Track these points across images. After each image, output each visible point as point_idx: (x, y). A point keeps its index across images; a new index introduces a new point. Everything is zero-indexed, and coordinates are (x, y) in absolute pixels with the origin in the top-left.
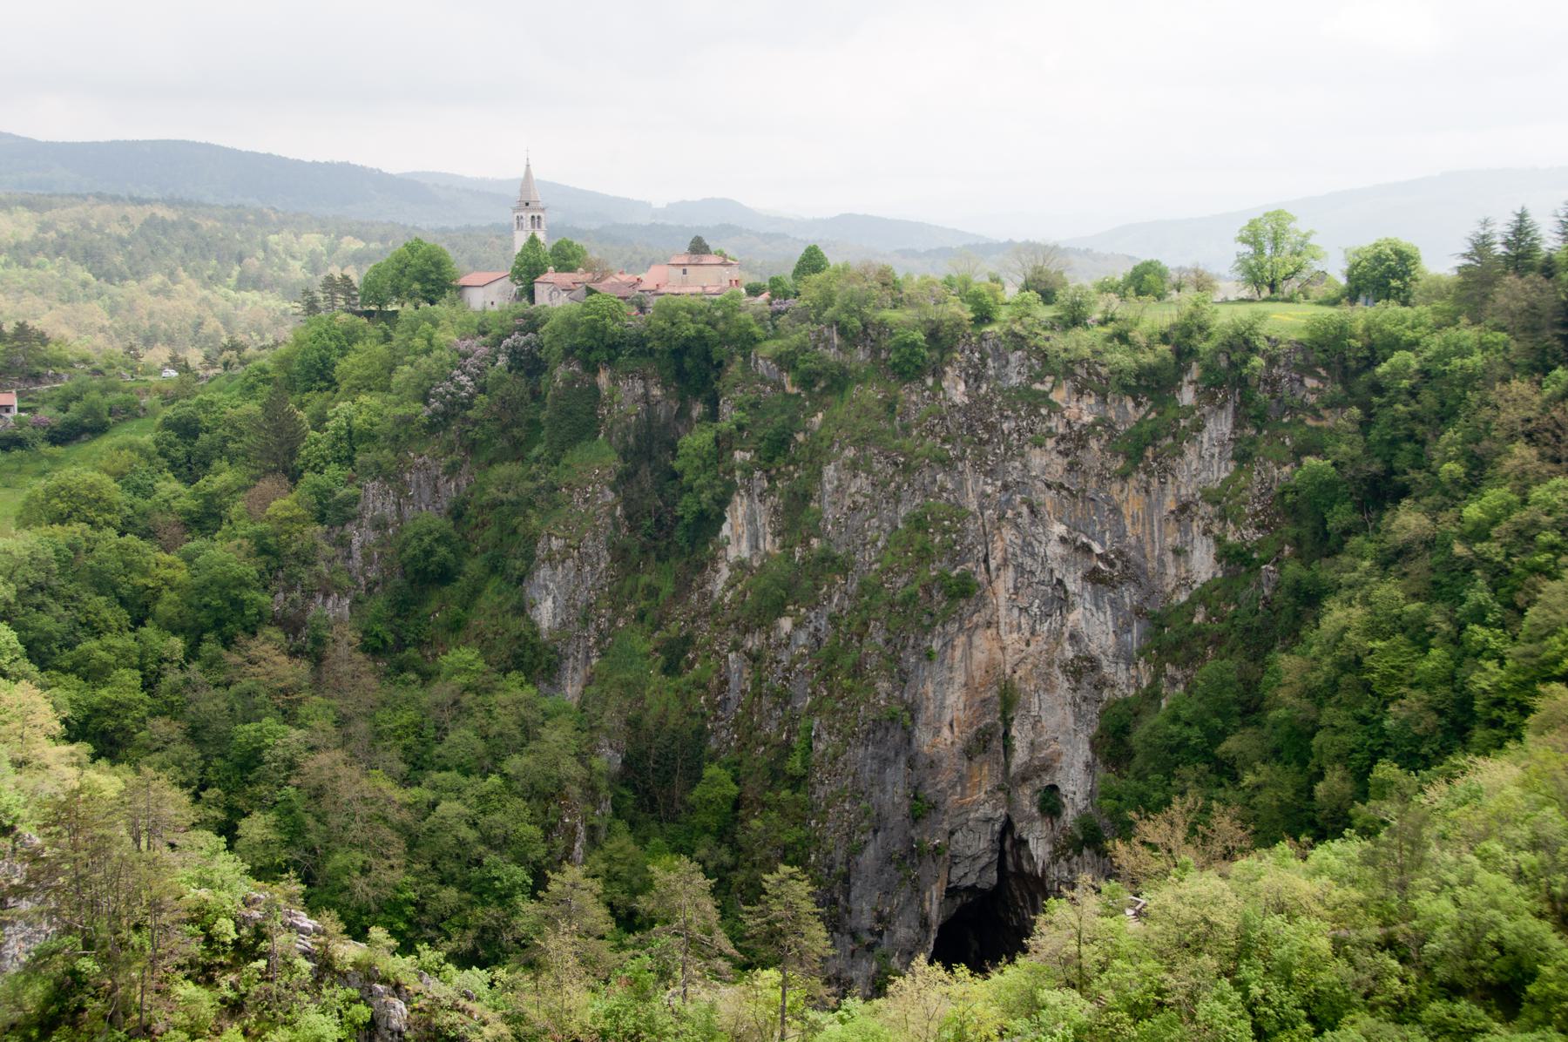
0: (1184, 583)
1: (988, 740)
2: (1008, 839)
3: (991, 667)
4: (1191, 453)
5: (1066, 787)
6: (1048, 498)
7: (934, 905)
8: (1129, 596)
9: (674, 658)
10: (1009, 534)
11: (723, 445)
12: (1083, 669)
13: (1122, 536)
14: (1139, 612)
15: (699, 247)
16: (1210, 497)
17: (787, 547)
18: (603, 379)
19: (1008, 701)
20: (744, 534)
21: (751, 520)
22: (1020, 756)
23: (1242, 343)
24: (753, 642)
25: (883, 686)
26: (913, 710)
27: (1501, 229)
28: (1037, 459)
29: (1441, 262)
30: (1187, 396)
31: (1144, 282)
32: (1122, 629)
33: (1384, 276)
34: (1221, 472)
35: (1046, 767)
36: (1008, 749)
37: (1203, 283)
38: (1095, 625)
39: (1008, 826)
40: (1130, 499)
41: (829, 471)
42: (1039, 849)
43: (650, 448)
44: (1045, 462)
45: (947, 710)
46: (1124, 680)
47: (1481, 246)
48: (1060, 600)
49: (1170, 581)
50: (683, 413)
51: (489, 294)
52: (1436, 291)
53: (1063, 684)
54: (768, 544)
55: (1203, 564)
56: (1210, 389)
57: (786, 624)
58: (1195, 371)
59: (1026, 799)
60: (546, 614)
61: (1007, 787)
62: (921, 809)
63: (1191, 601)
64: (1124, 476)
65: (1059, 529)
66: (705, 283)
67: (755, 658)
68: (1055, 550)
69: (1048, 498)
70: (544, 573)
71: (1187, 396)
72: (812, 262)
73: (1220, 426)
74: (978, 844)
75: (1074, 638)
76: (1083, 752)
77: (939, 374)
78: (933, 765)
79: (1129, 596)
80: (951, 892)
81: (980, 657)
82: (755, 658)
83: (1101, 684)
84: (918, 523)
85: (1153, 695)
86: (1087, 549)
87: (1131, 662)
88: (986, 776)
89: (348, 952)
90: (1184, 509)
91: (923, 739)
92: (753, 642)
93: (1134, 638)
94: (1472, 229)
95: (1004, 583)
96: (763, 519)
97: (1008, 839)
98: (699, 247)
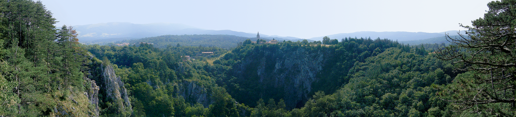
12: (310, 79)
20: (277, 66)
23: (324, 48)
28: (305, 59)
29: (340, 41)
33: (335, 42)
38: (311, 74)
40: (314, 62)
42: (306, 96)
45: (297, 82)
47: (343, 40)
52: (340, 43)
55: (321, 68)
60: (259, 73)
67: (278, 78)
72: (284, 41)
79: (314, 72)
82: (278, 78)
89: (240, 105)
90: (319, 64)
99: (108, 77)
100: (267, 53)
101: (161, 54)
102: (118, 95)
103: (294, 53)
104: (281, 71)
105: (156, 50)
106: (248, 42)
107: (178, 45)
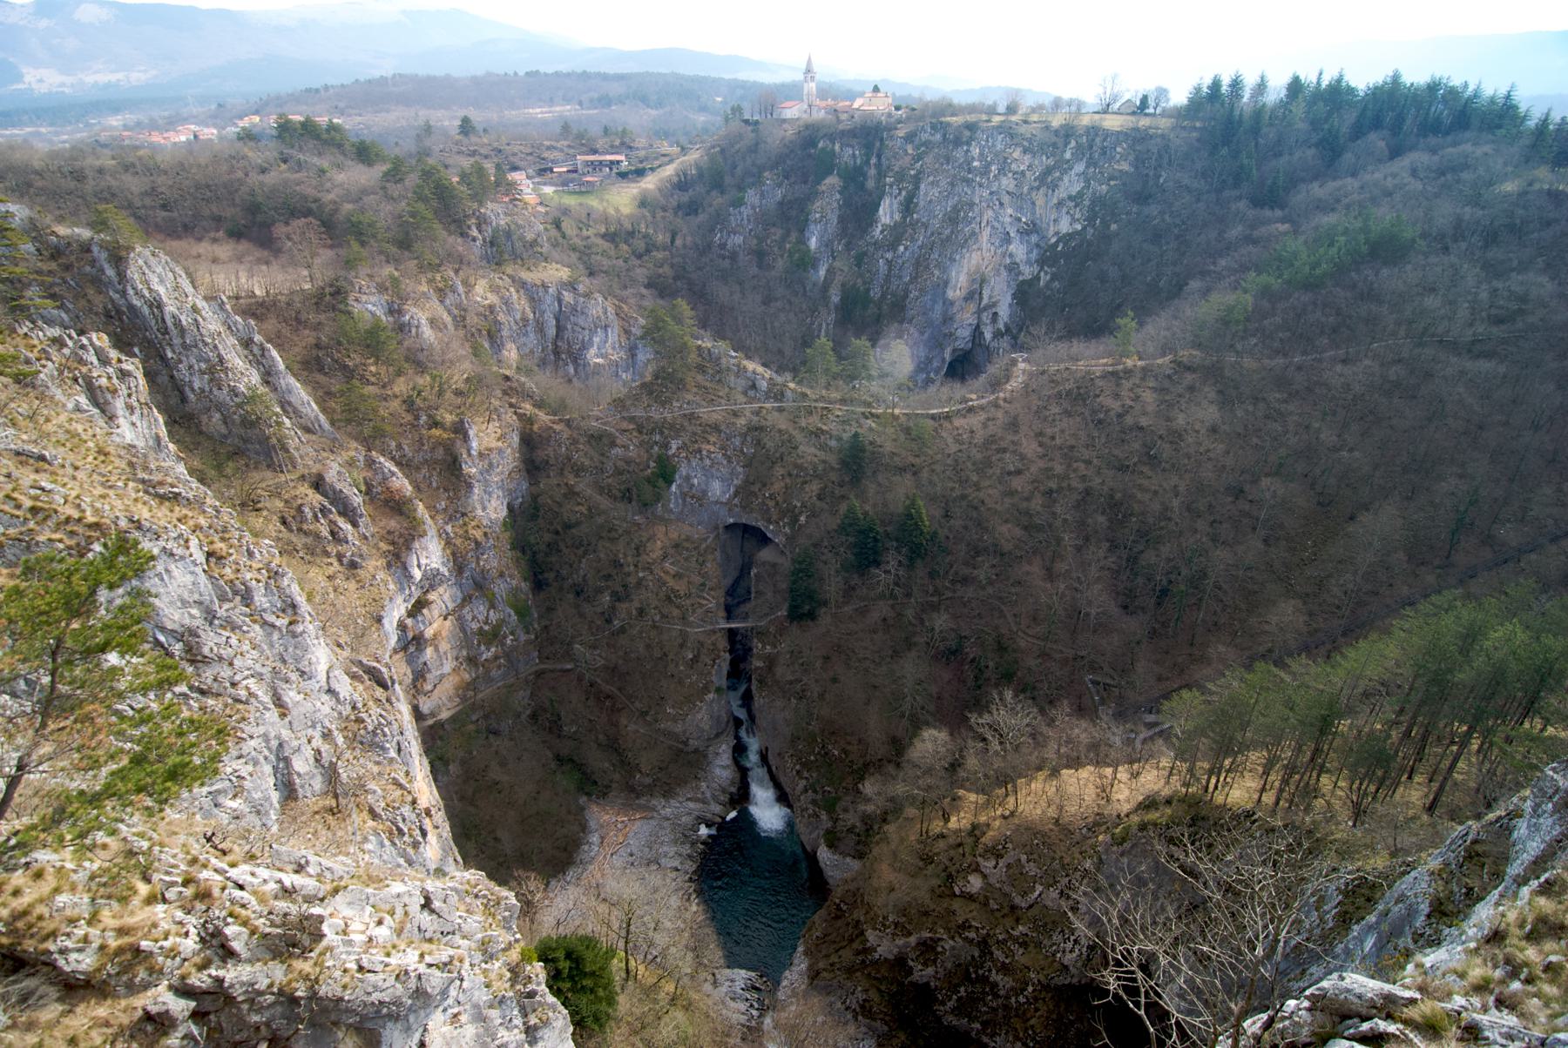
0: (1057, 233)
1: (973, 295)
2: (977, 331)
3: (978, 266)
4: (1066, 178)
5: (1001, 313)
6: (1006, 199)
7: (948, 356)
8: (1034, 238)
9: (860, 260)
10: (990, 213)
11: (881, 175)
12: (1013, 268)
13: (1034, 213)
14: (1038, 245)
15: (876, 89)
16: (1070, 198)
17: (904, 218)
18: (837, 147)
19: (983, 281)
20: (887, 213)
21: (891, 205)
22: (985, 301)
24: (889, 255)
25: (937, 272)
26: (946, 283)
27: (1208, 81)
30: (1068, 155)
31: (1057, 104)
32: (1030, 252)
34: (1076, 189)
35: (994, 305)
36: (981, 299)
37: (1080, 104)
38: (1018, 250)
39: (978, 326)
41: (922, 186)
42: (988, 336)
43: (853, 177)
44: (1007, 183)
45: (959, 281)
46: (1027, 272)
47: (1198, 89)
48: (1007, 239)
49: (1051, 233)
50: (867, 162)
51: (793, 111)
53: (1004, 273)
54: (897, 217)
56: (1080, 152)
57: (902, 248)
58: (1073, 143)
59: (986, 317)
60: (813, 243)
61: (979, 312)
62: (948, 319)
63: (1057, 242)
64: (1038, 189)
65: (1010, 211)
66: (880, 106)
67: (889, 262)
68: (1008, 220)
69: (1006, 199)
70: (812, 227)
71: (1068, 155)
73: (1080, 167)
74: (964, 333)
75: (1011, 255)
76: (1009, 299)
77: (968, 144)
78: (952, 303)
80: (954, 350)
81: (974, 262)
83: (1020, 273)
84: (954, 208)
85: (1038, 278)
86: (1019, 220)
87: (1031, 265)
88: (972, 307)
90: (1060, 204)
91: (950, 294)
92: (889, 255)
93: (1034, 255)
94: (1194, 82)
95: (987, 232)
96: (895, 206)
97: (977, 331)
98: (876, 89)
99: (160, 306)
100: (848, 155)
101: (395, 174)
102: (246, 377)
103: (959, 154)
104: (897, 234)
105: (364, 153)
106: (770, 99)
107: (466, 127)
